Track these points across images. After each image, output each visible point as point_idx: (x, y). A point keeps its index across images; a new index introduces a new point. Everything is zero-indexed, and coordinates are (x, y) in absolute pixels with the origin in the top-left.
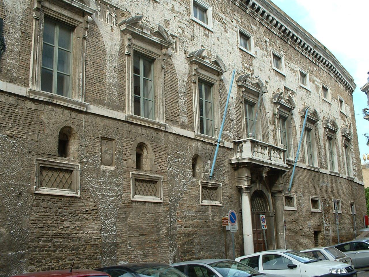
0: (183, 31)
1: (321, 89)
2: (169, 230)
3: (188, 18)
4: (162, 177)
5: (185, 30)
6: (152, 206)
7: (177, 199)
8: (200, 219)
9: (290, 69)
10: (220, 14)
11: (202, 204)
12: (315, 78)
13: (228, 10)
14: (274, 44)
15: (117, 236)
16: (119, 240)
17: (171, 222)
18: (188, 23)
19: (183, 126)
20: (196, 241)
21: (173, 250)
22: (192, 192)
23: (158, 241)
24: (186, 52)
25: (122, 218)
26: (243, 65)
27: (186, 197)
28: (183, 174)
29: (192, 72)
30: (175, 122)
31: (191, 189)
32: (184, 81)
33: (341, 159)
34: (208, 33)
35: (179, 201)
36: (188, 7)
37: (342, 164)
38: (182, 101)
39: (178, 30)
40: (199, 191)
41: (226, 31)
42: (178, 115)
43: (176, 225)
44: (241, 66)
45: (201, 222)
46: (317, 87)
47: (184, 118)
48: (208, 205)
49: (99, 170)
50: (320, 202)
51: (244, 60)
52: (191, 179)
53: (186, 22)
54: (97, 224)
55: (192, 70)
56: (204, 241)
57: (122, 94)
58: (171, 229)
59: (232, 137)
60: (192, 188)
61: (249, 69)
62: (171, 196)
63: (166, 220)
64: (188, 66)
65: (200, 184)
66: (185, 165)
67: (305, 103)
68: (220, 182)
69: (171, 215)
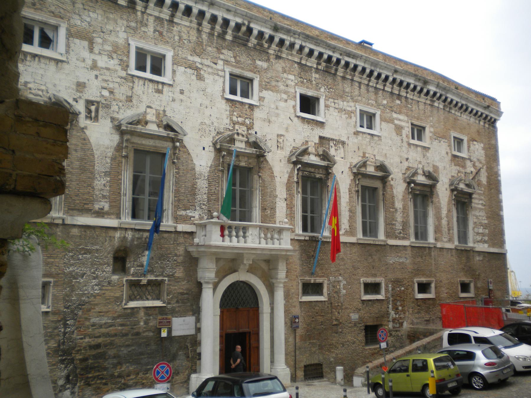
0: (111, 92)
1: (407, 130)
3: (123, 74)
4: (51, 280)
5: (115, 91)
7: (79, 305)
8: (122, 325)
9: (337, 111)
10: (190, 58)
11: (126, 307)
12: (395, 115)
13: (210, 49)
14: (305, 81)
18: (123, 80)
19: (100, 214)
21: (66, 367)
22: (108, 293)
24: (113, 119)
26: (231, 120)
27: (97, 300)
28: (94, 273)
29: (122, 143)
30: (85, 210)
31: (106, 290)
32: (106, 157)
33: (444, 222)
34: (163, 87)
35: (83, 307)
36: (125, 59)
37: (445, 229)
38: (101, 183)
39: (100, 93)
40: (123, 291)
41: (200, 78)
42: (92, 202)
43: (74, 336)
44: (228, 121)
45: (123, 329)
46: (399, 129)
47: (102, 203)
48: (139, 308)
50: (383, 286)
51: (235, 113)
53: (118, 80)
55: (123, 141)
56: (125, 352)
58: (64, 342)
59: (197, 217)
60: (110, 288)
61: (243, 124)
63: (56, 331)
64: (116, 138)
65: (125, 283)
66: (98, 261)
67: (364, 153)
68: (166, 277)
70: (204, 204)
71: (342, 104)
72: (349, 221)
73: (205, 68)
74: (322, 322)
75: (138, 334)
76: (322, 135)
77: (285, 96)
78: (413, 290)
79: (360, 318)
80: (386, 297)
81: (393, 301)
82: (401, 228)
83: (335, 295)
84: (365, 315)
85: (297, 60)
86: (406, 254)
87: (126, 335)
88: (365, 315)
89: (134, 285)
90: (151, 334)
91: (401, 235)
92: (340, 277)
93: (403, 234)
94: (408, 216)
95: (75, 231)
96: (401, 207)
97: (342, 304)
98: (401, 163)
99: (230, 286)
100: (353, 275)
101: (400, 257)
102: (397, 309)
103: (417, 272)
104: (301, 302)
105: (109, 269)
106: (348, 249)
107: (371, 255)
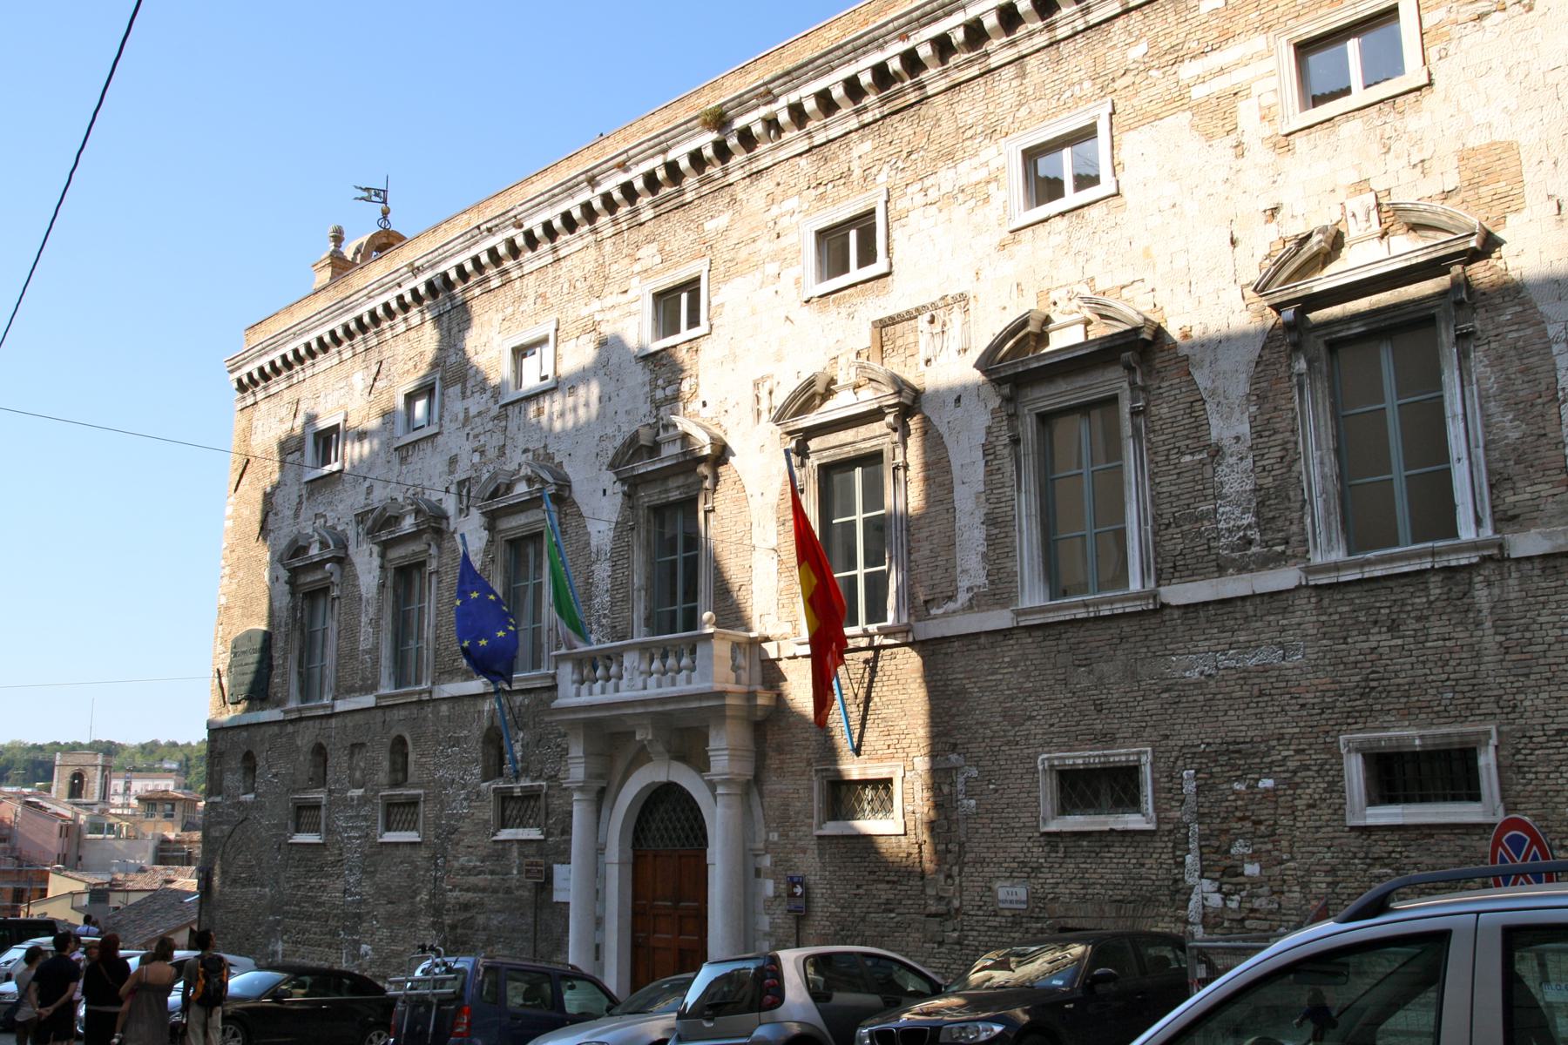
2: (432, 896)
6: (408, 850)
8: (492, 873)
15: (362, 902)
16: (364, 909)
17: (436, 879)
20: (481, 919)
23: (412, 914)
25: (368, 873)
44: (645, 408)
49: (345, 799)
50: (1147, 773)
52: (477, 785)
54: (340, 884)
57: (376, 662)
62: (438, 826)
69: (436, 865)
70: (605, 616)
71: (946, 178)
72: (985, 556)
73: (608, 315)
74: (888, 902)
75: (508, 891)
76: (883, 314)
77: (772, 269)
78: (1336, 786)
79: (1032, 896)
80: (1159, 821)
81: (1202, 837)
82: (1249, 519)
84: (1061, 889)
85: (803, 145)
86: (1283, 630)
87: (495, 891)
88: (1061, 889)
89: (504, 797)
90: (526, 894)
91: (1254, 549)
93: (1266, 544)
94: (1289, 457)
95: (444, 709)
96: (1245, 429)
98: (1233, 242)
99: (689, 794)
100: (1008, 743)
101: (1246, 647)
102: (1233, 871)
103: (1366, 699)
104: (820, 837)
105: (477, 770)
106: (983, 654)
107: (1087, 663)
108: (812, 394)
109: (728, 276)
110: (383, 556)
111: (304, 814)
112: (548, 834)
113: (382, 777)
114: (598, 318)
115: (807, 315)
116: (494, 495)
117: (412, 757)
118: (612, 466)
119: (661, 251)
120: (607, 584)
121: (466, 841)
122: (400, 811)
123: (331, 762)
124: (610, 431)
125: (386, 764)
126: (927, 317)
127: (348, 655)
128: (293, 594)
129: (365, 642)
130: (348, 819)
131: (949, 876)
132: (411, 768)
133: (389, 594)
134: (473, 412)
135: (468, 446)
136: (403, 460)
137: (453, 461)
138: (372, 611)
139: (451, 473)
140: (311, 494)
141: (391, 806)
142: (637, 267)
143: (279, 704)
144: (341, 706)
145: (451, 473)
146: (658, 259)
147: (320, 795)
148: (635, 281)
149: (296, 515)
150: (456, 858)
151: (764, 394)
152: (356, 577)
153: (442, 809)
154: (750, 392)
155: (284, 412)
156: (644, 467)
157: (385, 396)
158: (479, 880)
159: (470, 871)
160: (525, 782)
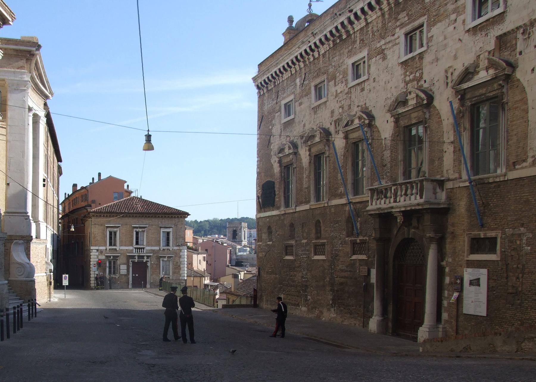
17: (331, 273)
44: (402, 85)
52: (345, 238)
57: (309, 192)
62: (332, 254)
77: (453, 17)
83: (513, 253)
89: (354, 243)
92: (522, 229)
97: (523, 266)
108: (468, 74)
109: (435, 23)
110: (310, 150)
111: (288, 250)
112: (369, 257)
113: (313, 235)
114: (383, 47)
115: (466, 38)
116: (347, 125)
117: (322, 228)
118: (389, 111)
119: (407, 15)
120: (389, 159)
121: (341, 260)
122: (319, 249)
123: (296, 230)
124: (389, 96)
125: (314, 231)
126: (521, 31)
127: (299, 190)
128: (281, 166)
129: (305, 186)
130: (302, 251)
131: (518, 278)
132: (322, 232)
133: (313, 166)
134: (339, 92)
135: (338, 105)
136: (315, 113)
137: (332, 112)
138: (307, 172)
139: (332, 117)
140: (284, 128)
141: (316, 246)
142: (398, 23)
143: (278, 208)
144: (299, 209)
145: (332, 117)
146: (406, 19)
147: (293, 242)
148: (397, 30)
149: (280, 136)
150: (338, 266)
151: (449, 75)
152: (301, 160)
153: (333, 247)
154: (443, 74)
155: (274, 96)
156: (401, 110)
157: (308, 87)
158: (346, 274)
159: (342, 271)
160: (361, 238)
